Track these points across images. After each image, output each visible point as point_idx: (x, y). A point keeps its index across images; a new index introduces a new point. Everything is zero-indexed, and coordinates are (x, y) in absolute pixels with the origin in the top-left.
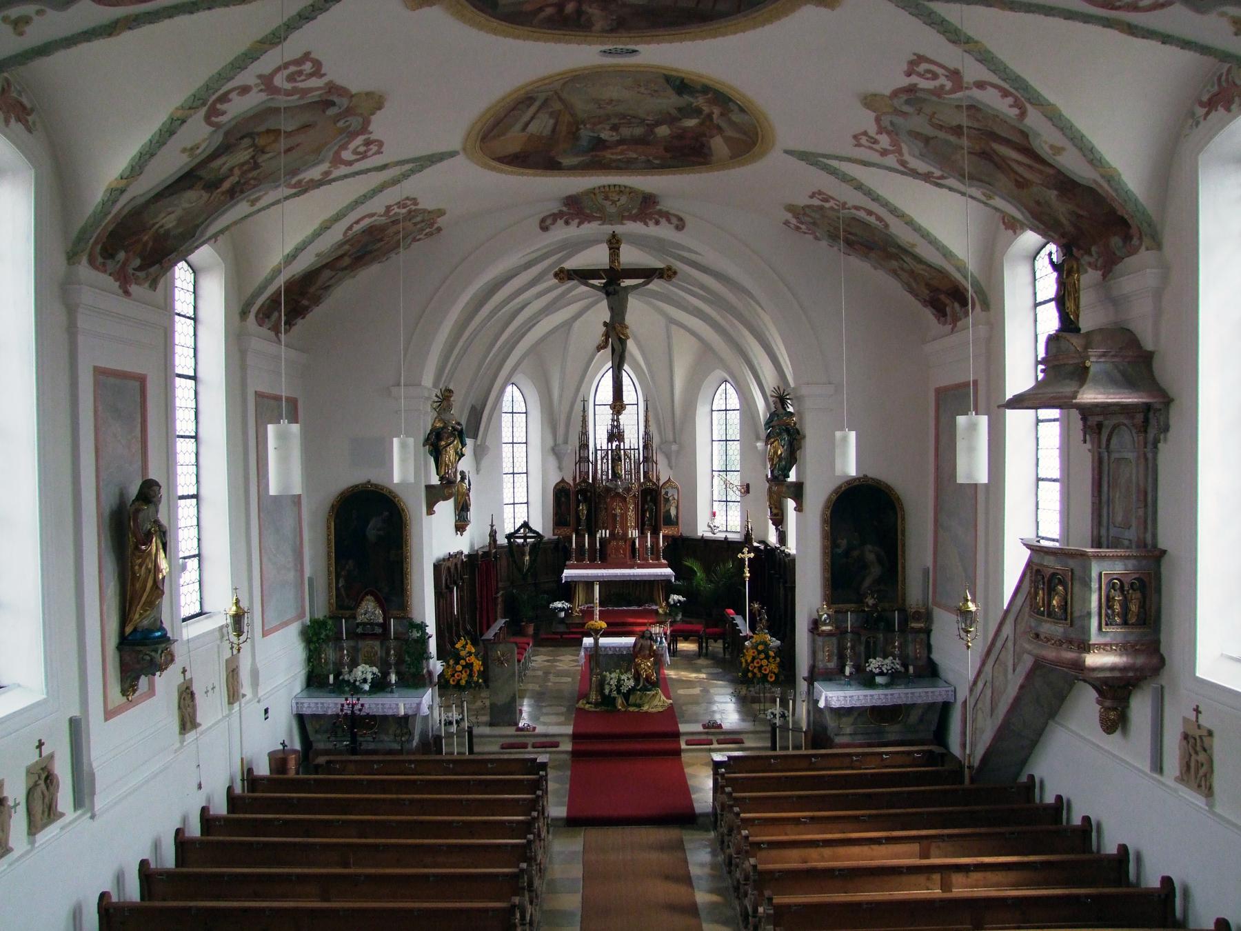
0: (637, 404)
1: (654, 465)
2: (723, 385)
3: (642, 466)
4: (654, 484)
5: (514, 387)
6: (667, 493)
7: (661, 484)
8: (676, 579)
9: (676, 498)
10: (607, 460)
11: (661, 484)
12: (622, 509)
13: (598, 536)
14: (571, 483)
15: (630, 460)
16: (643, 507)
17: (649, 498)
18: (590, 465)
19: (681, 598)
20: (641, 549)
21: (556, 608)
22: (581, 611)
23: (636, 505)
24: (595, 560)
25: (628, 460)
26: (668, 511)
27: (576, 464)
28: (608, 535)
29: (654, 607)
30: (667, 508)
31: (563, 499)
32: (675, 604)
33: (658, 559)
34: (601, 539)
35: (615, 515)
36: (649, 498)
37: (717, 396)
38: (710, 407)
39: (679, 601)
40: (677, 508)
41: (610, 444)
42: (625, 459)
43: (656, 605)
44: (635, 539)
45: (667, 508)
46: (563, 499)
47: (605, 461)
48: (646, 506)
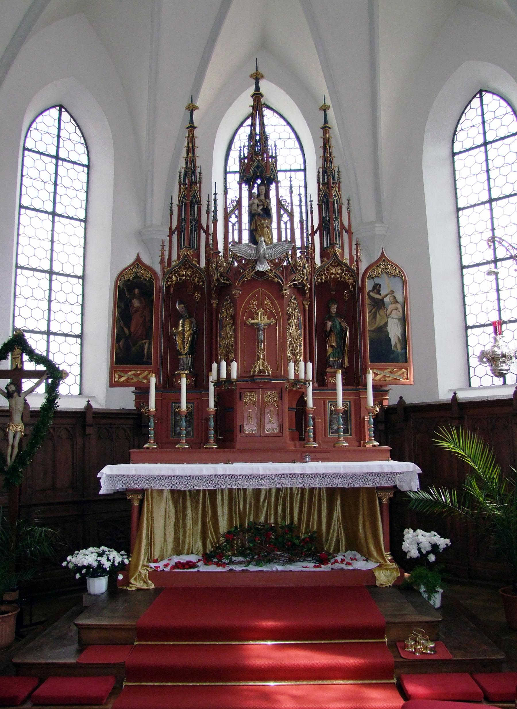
0: (304, 170)
1: (346, 236)
2: (476, 102)
3: (317, 236)
4: (349, 269)
5: (65, 116)
6: (377, 288)
7: (363, 267)
8: (424, 486)
9: (399, 297)
10: (239, 217)
11: (363, 267)
12: (271, 315)
13: (213, 377)
14: (157, 268)
15: (291, 215)
16: (322, 325)
17: (334, 309)
18: (203, 236)
19: (443, 542)
20: (319, 420)
21: (78, 569)
22: (154, 575)
23: (307, 314)
24: (207, 442)
25: (285, 218)
26: (382, 330)
27: (171, 233)
28: (234, 375)
29: (361, 565)
30: (380, 321)
31: (136, 303)
32: (423, 556)
33: (360, 437)
34: (218, 383)
35: (255, 328)
36: (334, 309)
37: (465, 123)
38: (449, 146)
39: (435, 547)
40: (403, 320)
41: (245, 187)
42: (279, 217)
43: (368, 557)
44: (305, 382)
45: (380, 321)
46: (136, 303)
47: (233, 219)
48: (329, 324)
